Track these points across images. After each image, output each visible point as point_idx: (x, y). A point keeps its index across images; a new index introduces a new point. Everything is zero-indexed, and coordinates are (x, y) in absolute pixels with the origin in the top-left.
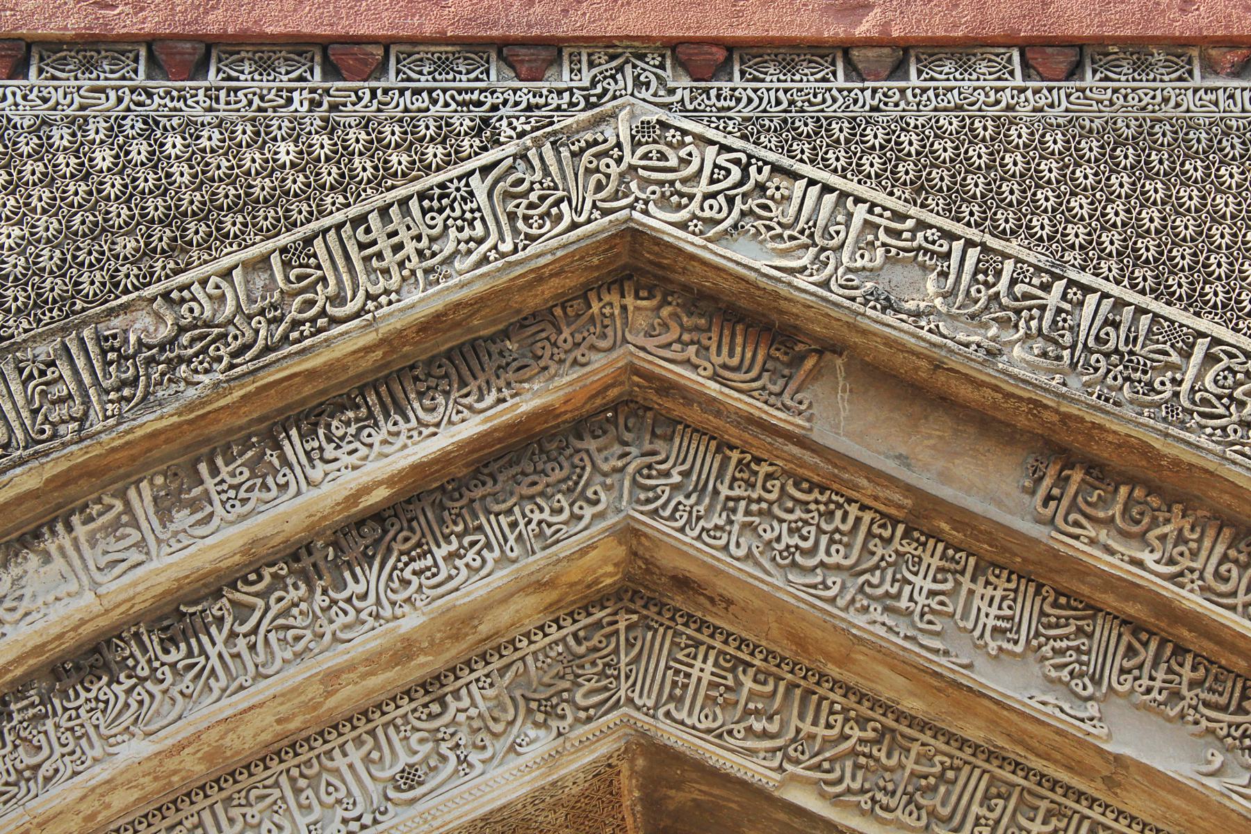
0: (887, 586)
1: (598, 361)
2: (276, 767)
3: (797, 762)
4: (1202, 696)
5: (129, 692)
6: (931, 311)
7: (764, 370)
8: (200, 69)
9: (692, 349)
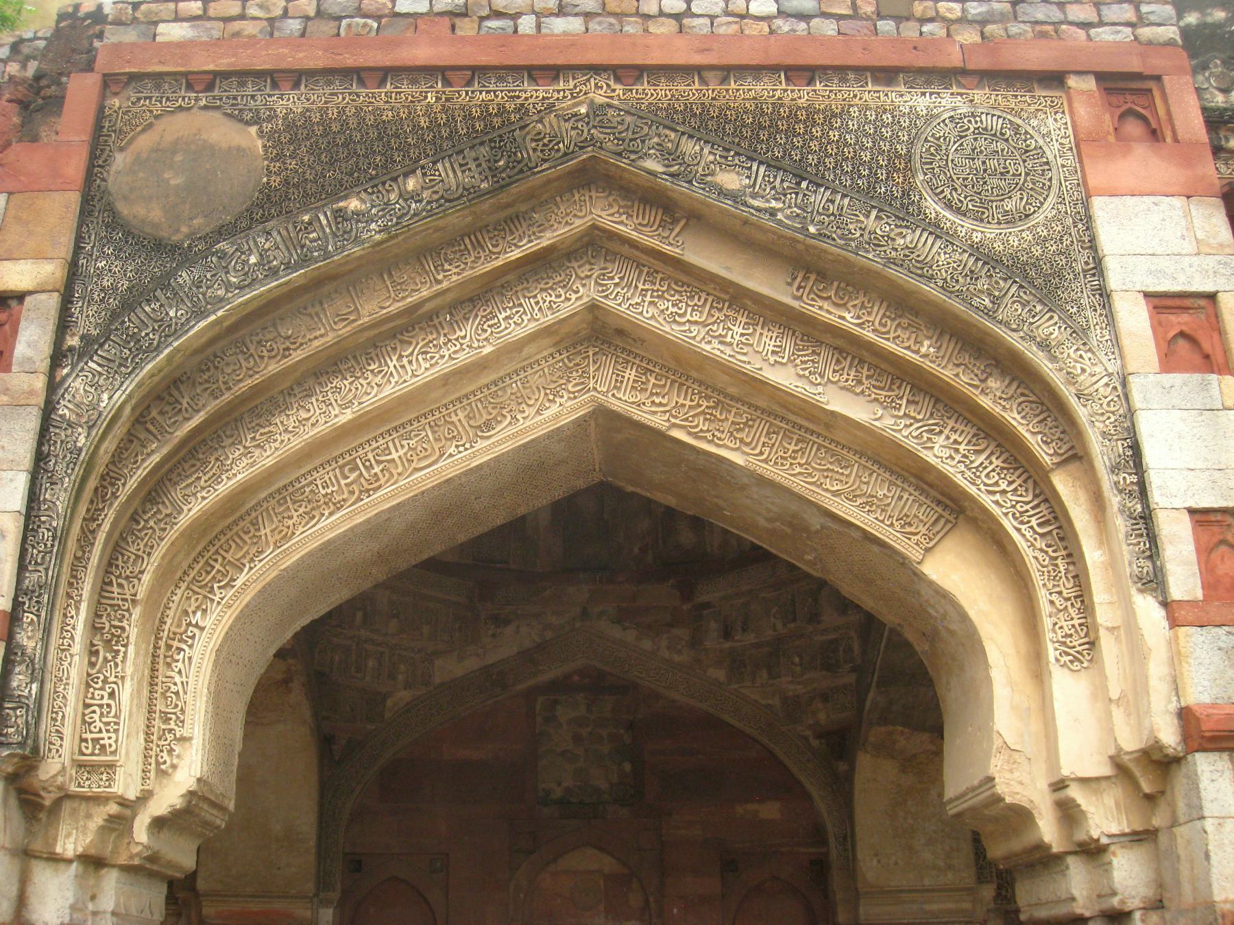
0: (720, 331)
1: (578, 222)
2: (423, 421)
3: (676, 417)
4: (873, 382)
5: (351, 383)
7: (659, 226)
9: (624, 217)
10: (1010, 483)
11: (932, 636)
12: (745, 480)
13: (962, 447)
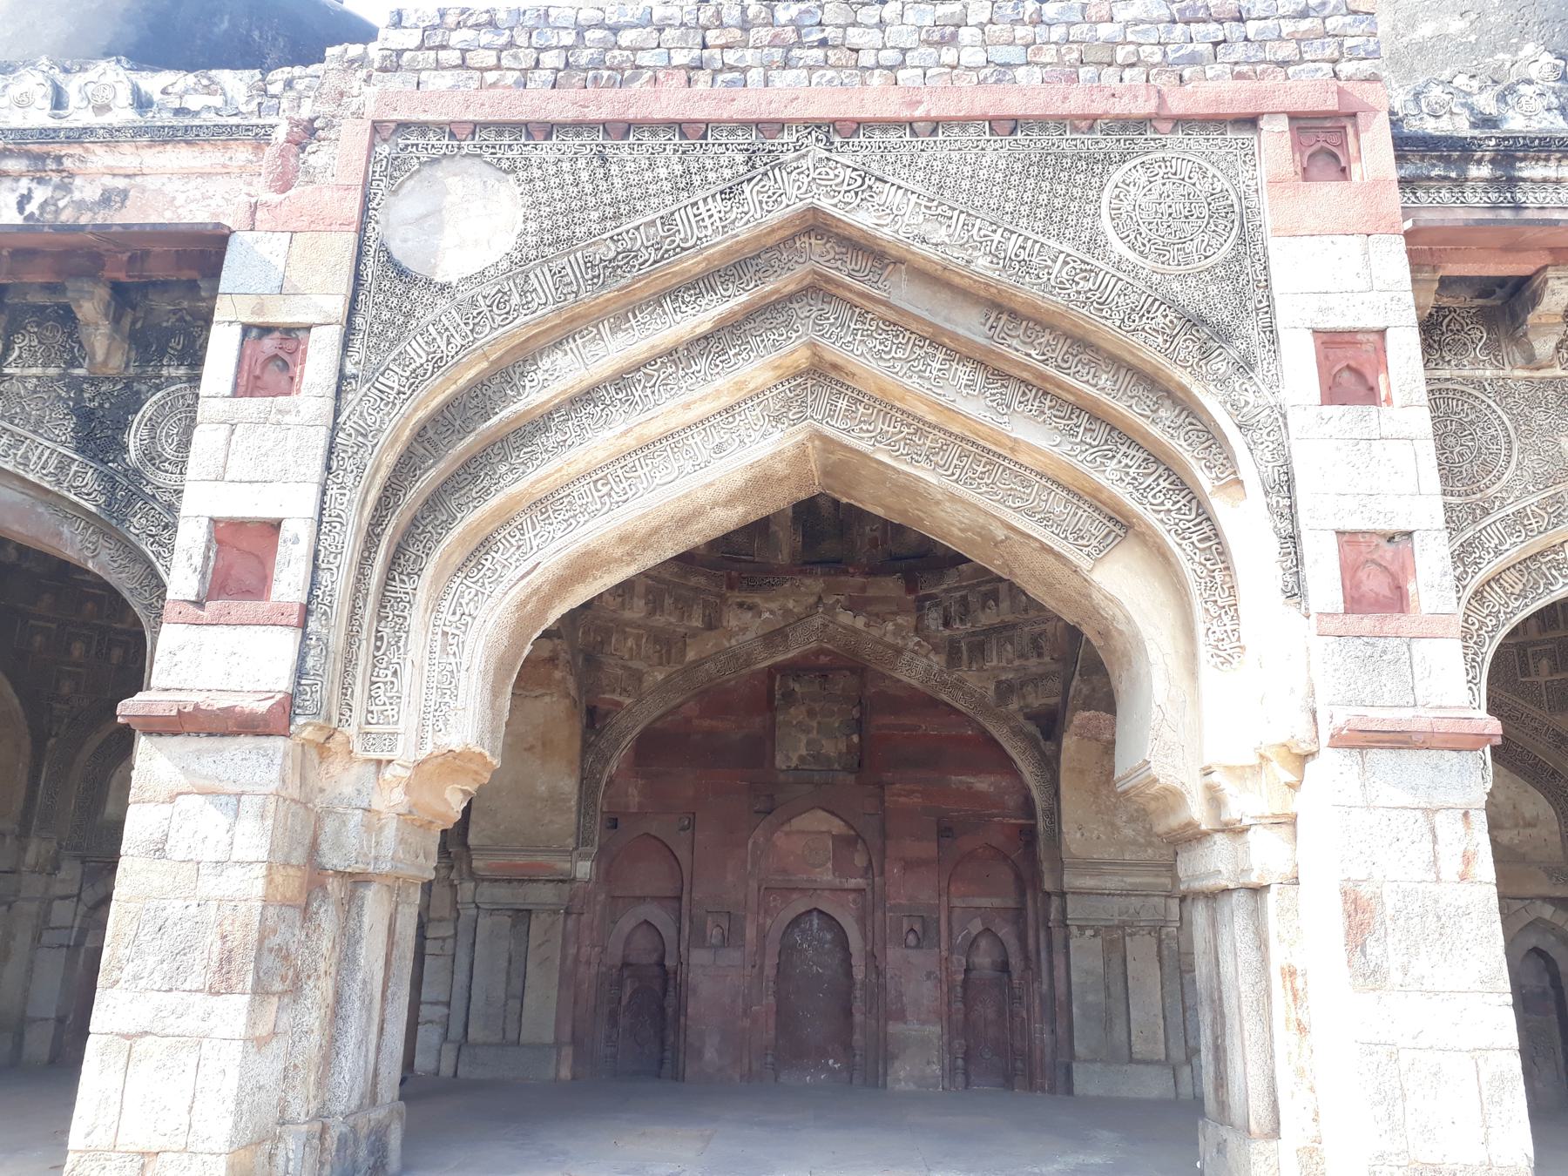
6: (943, 243)
8: (626, 135)
10: (1175, 503)
11: (1105, 634)
12: (939, 497)
13: (1131, 471)
